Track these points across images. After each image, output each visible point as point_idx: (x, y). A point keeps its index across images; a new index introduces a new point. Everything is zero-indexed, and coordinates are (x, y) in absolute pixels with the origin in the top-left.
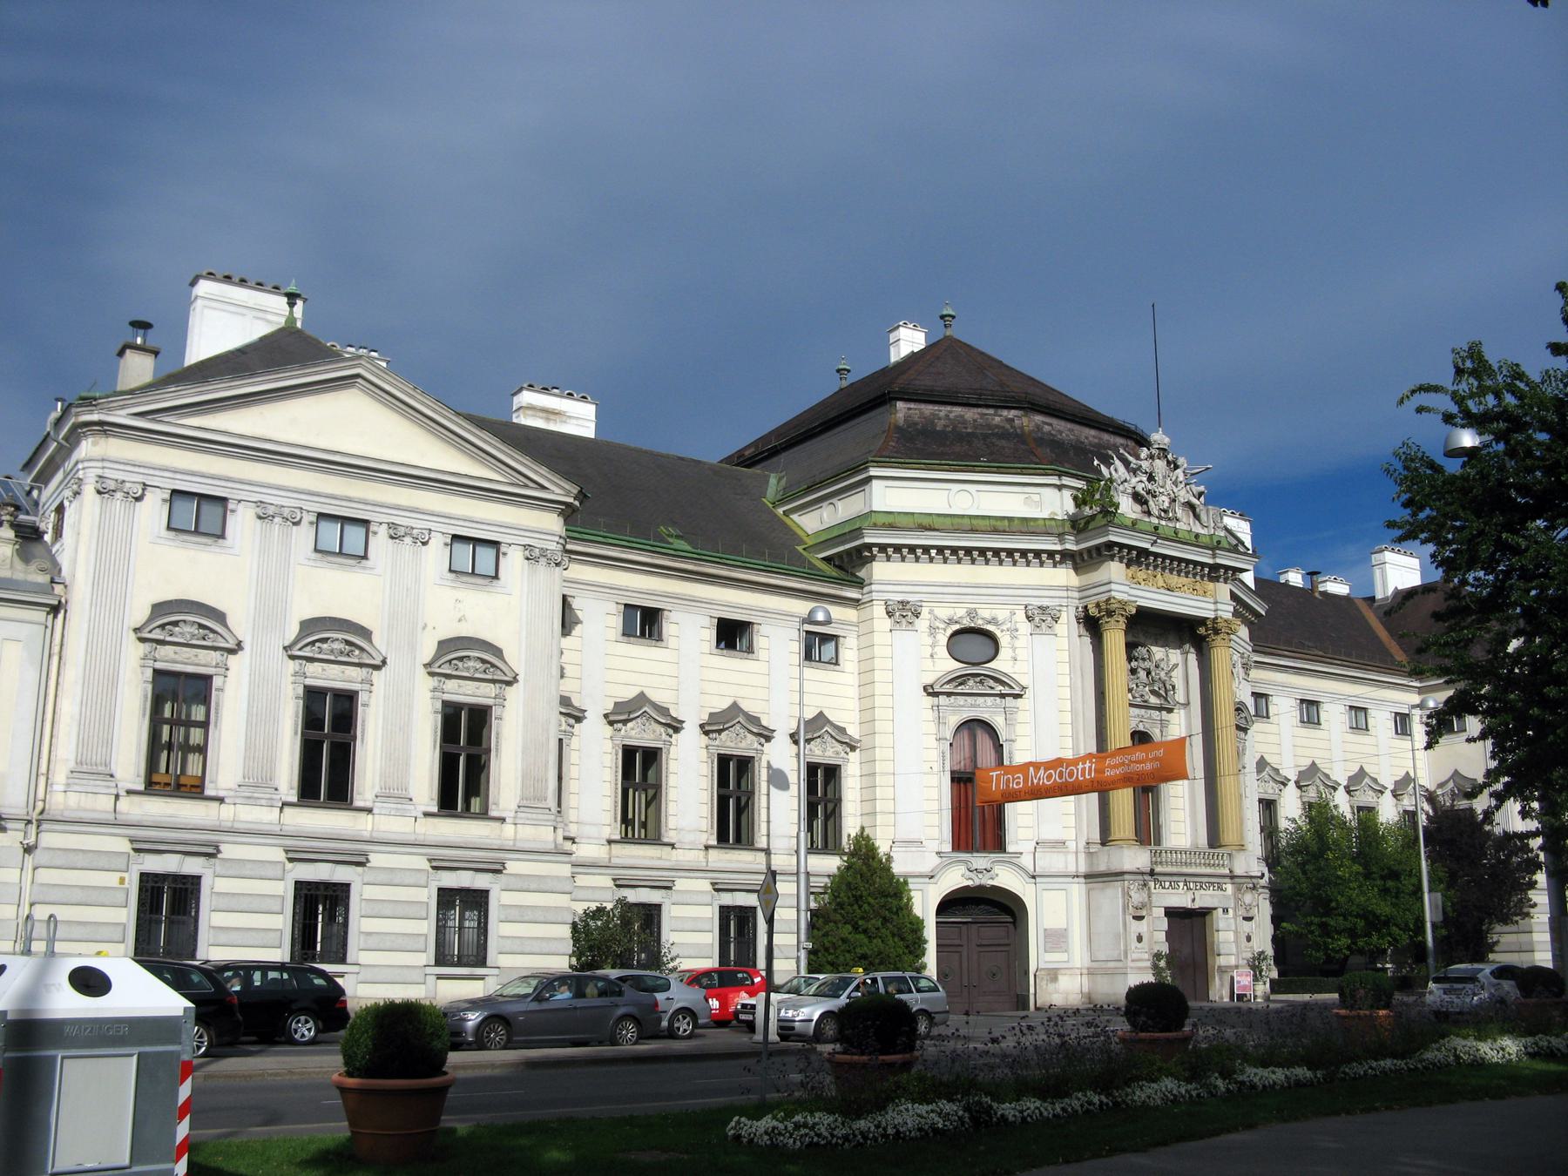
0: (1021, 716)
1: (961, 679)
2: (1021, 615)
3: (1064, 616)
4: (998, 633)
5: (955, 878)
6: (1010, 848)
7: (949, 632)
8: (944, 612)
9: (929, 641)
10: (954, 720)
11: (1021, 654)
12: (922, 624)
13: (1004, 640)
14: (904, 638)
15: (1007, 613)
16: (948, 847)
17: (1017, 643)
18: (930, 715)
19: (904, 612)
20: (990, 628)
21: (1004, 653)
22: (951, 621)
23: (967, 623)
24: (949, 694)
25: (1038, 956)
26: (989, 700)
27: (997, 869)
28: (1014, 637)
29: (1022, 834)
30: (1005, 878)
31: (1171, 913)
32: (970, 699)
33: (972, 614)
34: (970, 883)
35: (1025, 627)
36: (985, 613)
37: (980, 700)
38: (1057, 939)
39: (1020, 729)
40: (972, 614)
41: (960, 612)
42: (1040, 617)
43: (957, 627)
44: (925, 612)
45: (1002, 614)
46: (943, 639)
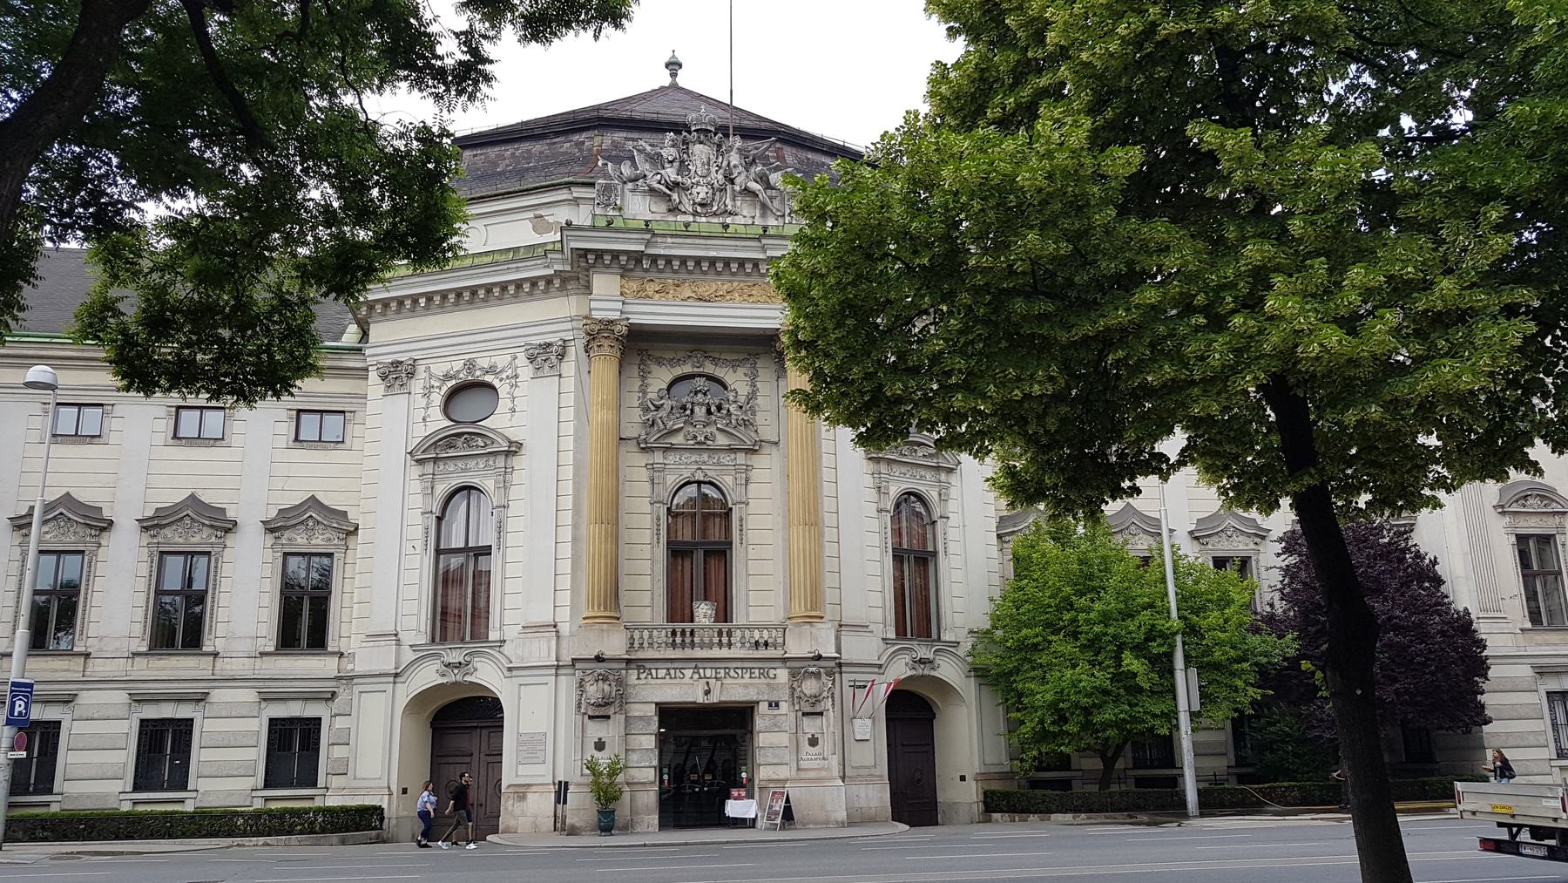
0: (516, 477)
1: (449, 441)
2: (522, 359)
3: (571, 351)
4: (496, 383)
5: (428, 676)
6: (493, 635)
7: (445, 389)
8: (439, 368)
10: (442, 489)
12: (417, 385)
15: (509, 358)
16: (423, 639)
18: (416, 486)
19: (398, 374)
20: (488, 378)
21: (504, 404)
22: (447, 377)
24: (436, 460)
25: (510, 773)
27: (478, 663)
30: (487, 675)
32: (460, 464)
33: (470, 365)
34: (444, 680)
35: (526, 371)
36: (484, 363)
37: (472, 463)
38: (533, 746)
39: (514, 492)
40: (470, 365)
42: (546, 356)
44: (421, 369)
45: (502, 361)
46: (437, 398)
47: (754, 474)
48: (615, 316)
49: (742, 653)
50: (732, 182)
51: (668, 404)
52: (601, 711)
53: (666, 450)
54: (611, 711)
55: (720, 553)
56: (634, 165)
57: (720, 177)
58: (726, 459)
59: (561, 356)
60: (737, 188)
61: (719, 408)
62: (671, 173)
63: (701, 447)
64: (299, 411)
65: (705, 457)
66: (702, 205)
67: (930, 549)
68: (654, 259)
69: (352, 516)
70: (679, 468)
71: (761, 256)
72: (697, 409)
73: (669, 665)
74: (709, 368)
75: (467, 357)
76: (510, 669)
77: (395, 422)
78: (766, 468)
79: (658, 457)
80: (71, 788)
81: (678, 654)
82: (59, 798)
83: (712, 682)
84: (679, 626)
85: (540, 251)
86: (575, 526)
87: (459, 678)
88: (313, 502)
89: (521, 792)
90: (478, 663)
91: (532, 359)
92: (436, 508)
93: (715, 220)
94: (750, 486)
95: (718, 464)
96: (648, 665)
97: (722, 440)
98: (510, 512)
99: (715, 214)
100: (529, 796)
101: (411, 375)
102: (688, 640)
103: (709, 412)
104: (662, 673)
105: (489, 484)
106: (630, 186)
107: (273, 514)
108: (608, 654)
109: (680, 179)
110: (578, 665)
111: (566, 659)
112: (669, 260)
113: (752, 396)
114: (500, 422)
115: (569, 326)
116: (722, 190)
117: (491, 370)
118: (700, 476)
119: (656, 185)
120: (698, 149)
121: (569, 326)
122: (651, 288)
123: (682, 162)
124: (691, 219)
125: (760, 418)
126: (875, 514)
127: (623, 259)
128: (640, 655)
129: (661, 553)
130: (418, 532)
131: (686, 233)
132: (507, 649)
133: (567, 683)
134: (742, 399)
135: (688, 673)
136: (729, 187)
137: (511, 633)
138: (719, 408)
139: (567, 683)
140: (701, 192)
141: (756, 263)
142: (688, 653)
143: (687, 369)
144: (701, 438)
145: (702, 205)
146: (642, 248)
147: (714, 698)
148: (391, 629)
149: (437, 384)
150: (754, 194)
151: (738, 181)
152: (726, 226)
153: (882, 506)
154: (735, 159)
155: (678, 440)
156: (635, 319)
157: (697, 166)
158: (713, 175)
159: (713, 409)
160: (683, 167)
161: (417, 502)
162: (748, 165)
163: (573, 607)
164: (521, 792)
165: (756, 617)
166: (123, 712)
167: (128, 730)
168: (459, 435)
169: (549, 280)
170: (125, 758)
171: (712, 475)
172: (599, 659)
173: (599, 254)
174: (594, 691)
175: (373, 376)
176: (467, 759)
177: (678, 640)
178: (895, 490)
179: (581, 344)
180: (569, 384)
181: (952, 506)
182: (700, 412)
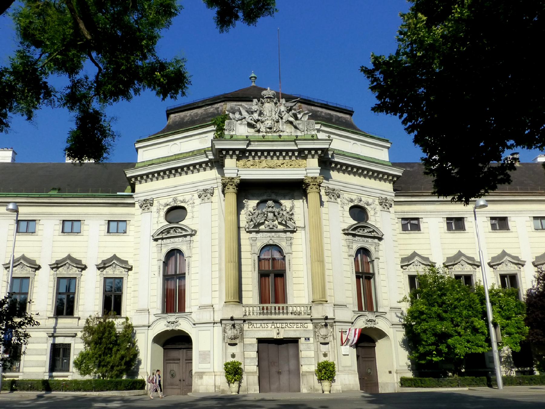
0: (194, 245)
1: (168, 231)
3: (216, 192)
4: (186, 206)
8: (163, 201)
9: (155, 215)
10: (165, 250)
11: (195, 214)
12: (154, 209)
13: (189, 209)
14: (147, 216)
17: (195, 209)
18: (155, 249)
19: (147, 204)
20: (182, 205)
23: (173, 204)
24: (162, 239)
25: (197, 366)
26: (181, 239)
27: (181, 321)
28: (193, 207)
29: (193, 303)
31: (261, 341)
32: (172, 240)
33: (175, 200)
35: (198, 201)
36: (181, 198)
37: (177, 239)
39: (194, 251)
40: (175, 200)
41: (170, 200)
42: (206, 194)
43: (169, 207)
44: (155, 203)
45: (187, 197)
46: (163, 213)
47: (294, 241)
48: (234, 176)
49: (293, 316)
50: (282, 118)
51: (257, 212)
52: (233, 342)
53: (257, 232)
54: (237, 341)
55: (281, 275)
56: (241, 114)
57: (277, 117)
58: (282, 235)
59: (212, 194)
60: (284, 121)
61: (279, 214)
62: (256, 116)
63: (271, 231)
64: (109, 221)
65: (273, 234)
66: (270, 128)
67: (371, 271)
68: (250, 151)
69: (131, 263)
70: (263, 239)
71: (296, 148)
72: (269, 214)
73: (261, 322)
74: (274, 197)
75: (174, 196)
76: (194, 324)
77: (145, 223)
78: (300, 237)
79: (254, 234)
80: (26, 370)
81: (265, 317)
82: (22, 374)
83: (280, 329)
84: (265, 305)
85: (203, 151)
86: (220, 264)
87: (174, 328)
88: (115, 257)
89: (201, 375)
90: (181, 321)
91: (200, 197)
92: (163, 259)
93: (275, 134)
94: (293, 246)
95: (279, 237)
96: (252, 322)
97: (281, 227)
98: (193, 259)
99: (275, 132)
100: (204, 377)
101: (152, 205)
102: (269, 311)
103: (275, 215)
104: (259, 325)
105: (184, 248)
106: (239, 122)
107: (100, 262)
108: (235, 317)
109: (260, 118)
110: (223, 322)
111: (218, 319)
112: (256, 151)
113: (292, 208)
114: (186, 222)
115: (215, 181)
116: (278, 122)
117: (183, 201)
118: (271, 242)
119: (250, 121)
120: (267, 105)
121: (215, 181)
122: (249, 164)
123: (260, 111)
124: (265, 134)
125: (295, 217)
126: (347, 257)
127: (237, 152)
128: (249, 317)
129: (256, 275)
130: (156, 268)
131: (264, 140)
132: (193, 316)
133: (218, 329)
134: (288, 210)
135: (270, 325)
136: (280, 121)
137: (194, 309)
138: (279, 214)
139: (218, 329)
140: (269, 123)
141: (293, 151)
142: (269, 317)
143: (265, 197)
144: (271, 226)
145: (270, 128)
146: (245, 147)
147: (281, 336)
148: (146, 307)
149: (162, 208)
150: (291, 123)
151: (284, 118)
152: (280, 136)
153: (350, 253)
154: (283, 108)
155: (262, 227)
156: (243, 177)
157: (266, 112)
158: (274, 115)
159: (276, 214)
160: (261, 114)
161: (155, 255)
162: (289, 110)
163: (220, 298)
164: (201, 375)
165: (297, 301)
166: (45, 340)
167: (47, 347)
168: (172, 228)
169: (206, 163)
170: (46, 358)
171: (277, 242)
172: (232, 319)
173: (227, 150)
174: (231, 333)
175: (137, 205)
176: (178, 361)
177: (265, 311)
178: (355, 247)
179: (220, 188)
180: (215, 205)
181: (380, 254)
182: (271, 215)
